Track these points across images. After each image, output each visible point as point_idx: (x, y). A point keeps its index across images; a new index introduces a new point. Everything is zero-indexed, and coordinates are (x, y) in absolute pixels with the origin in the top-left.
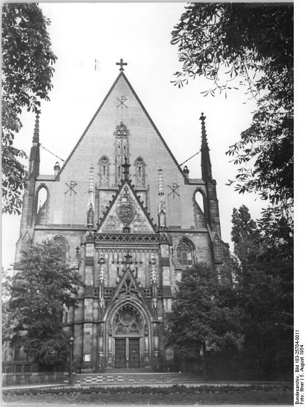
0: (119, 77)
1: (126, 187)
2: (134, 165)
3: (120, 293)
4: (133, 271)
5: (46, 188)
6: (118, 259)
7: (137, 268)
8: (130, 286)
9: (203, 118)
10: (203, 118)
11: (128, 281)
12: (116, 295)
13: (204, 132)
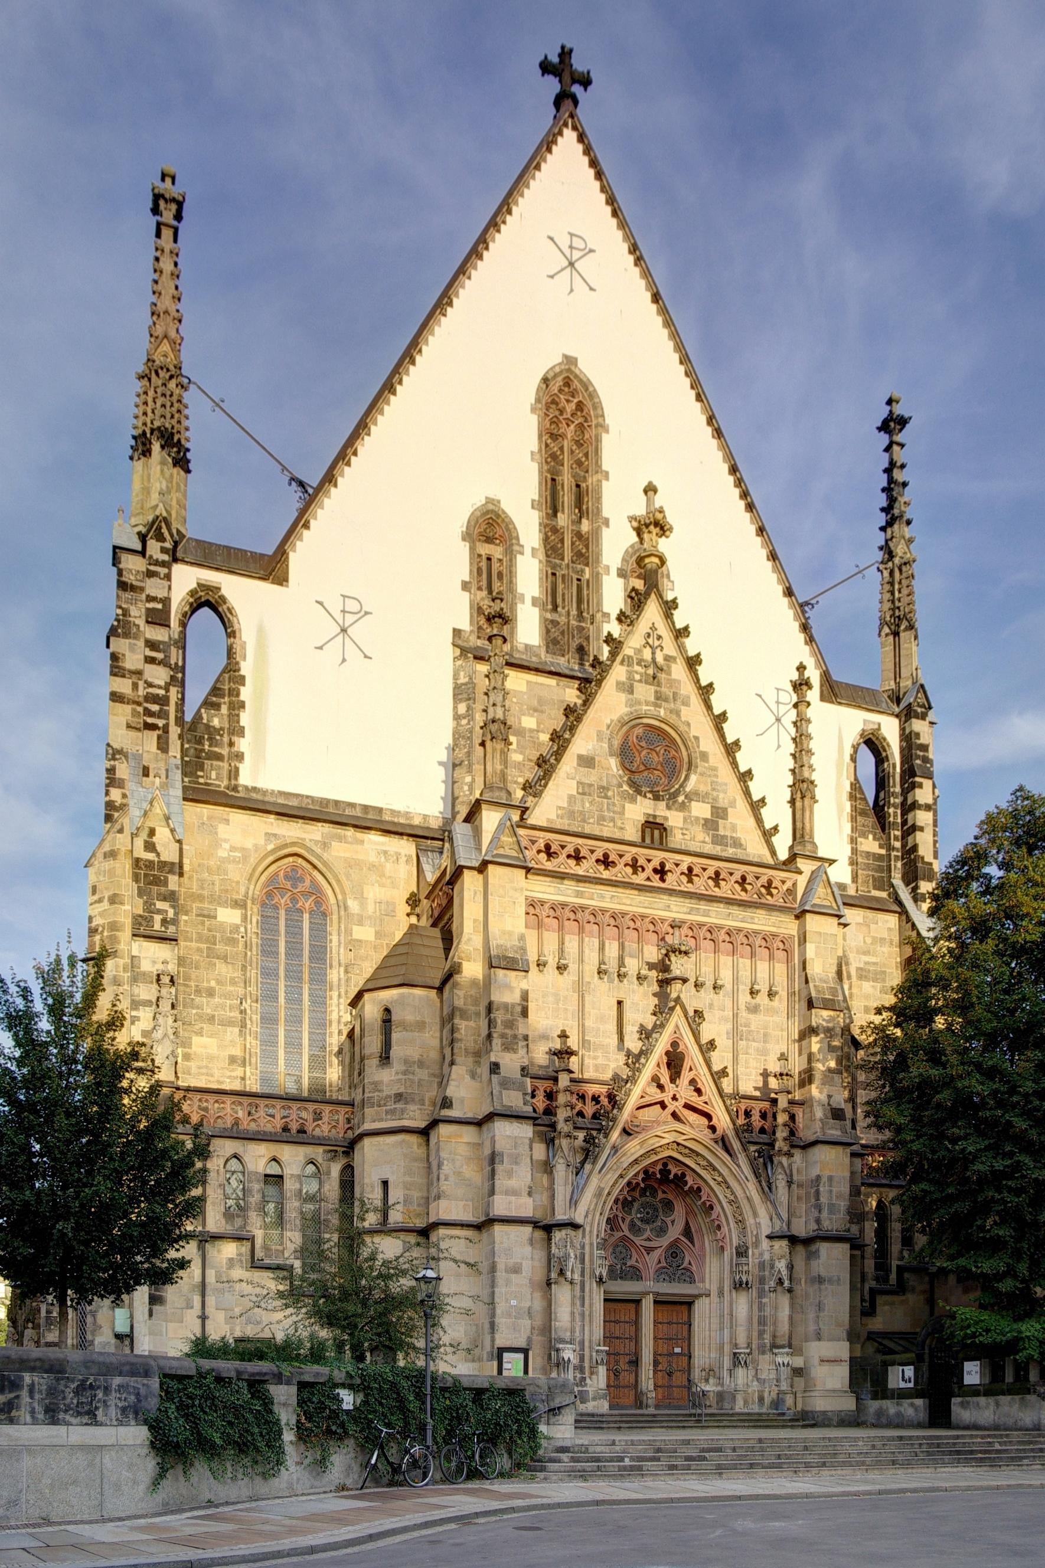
6: (621, 963)
11: (674, 1061)
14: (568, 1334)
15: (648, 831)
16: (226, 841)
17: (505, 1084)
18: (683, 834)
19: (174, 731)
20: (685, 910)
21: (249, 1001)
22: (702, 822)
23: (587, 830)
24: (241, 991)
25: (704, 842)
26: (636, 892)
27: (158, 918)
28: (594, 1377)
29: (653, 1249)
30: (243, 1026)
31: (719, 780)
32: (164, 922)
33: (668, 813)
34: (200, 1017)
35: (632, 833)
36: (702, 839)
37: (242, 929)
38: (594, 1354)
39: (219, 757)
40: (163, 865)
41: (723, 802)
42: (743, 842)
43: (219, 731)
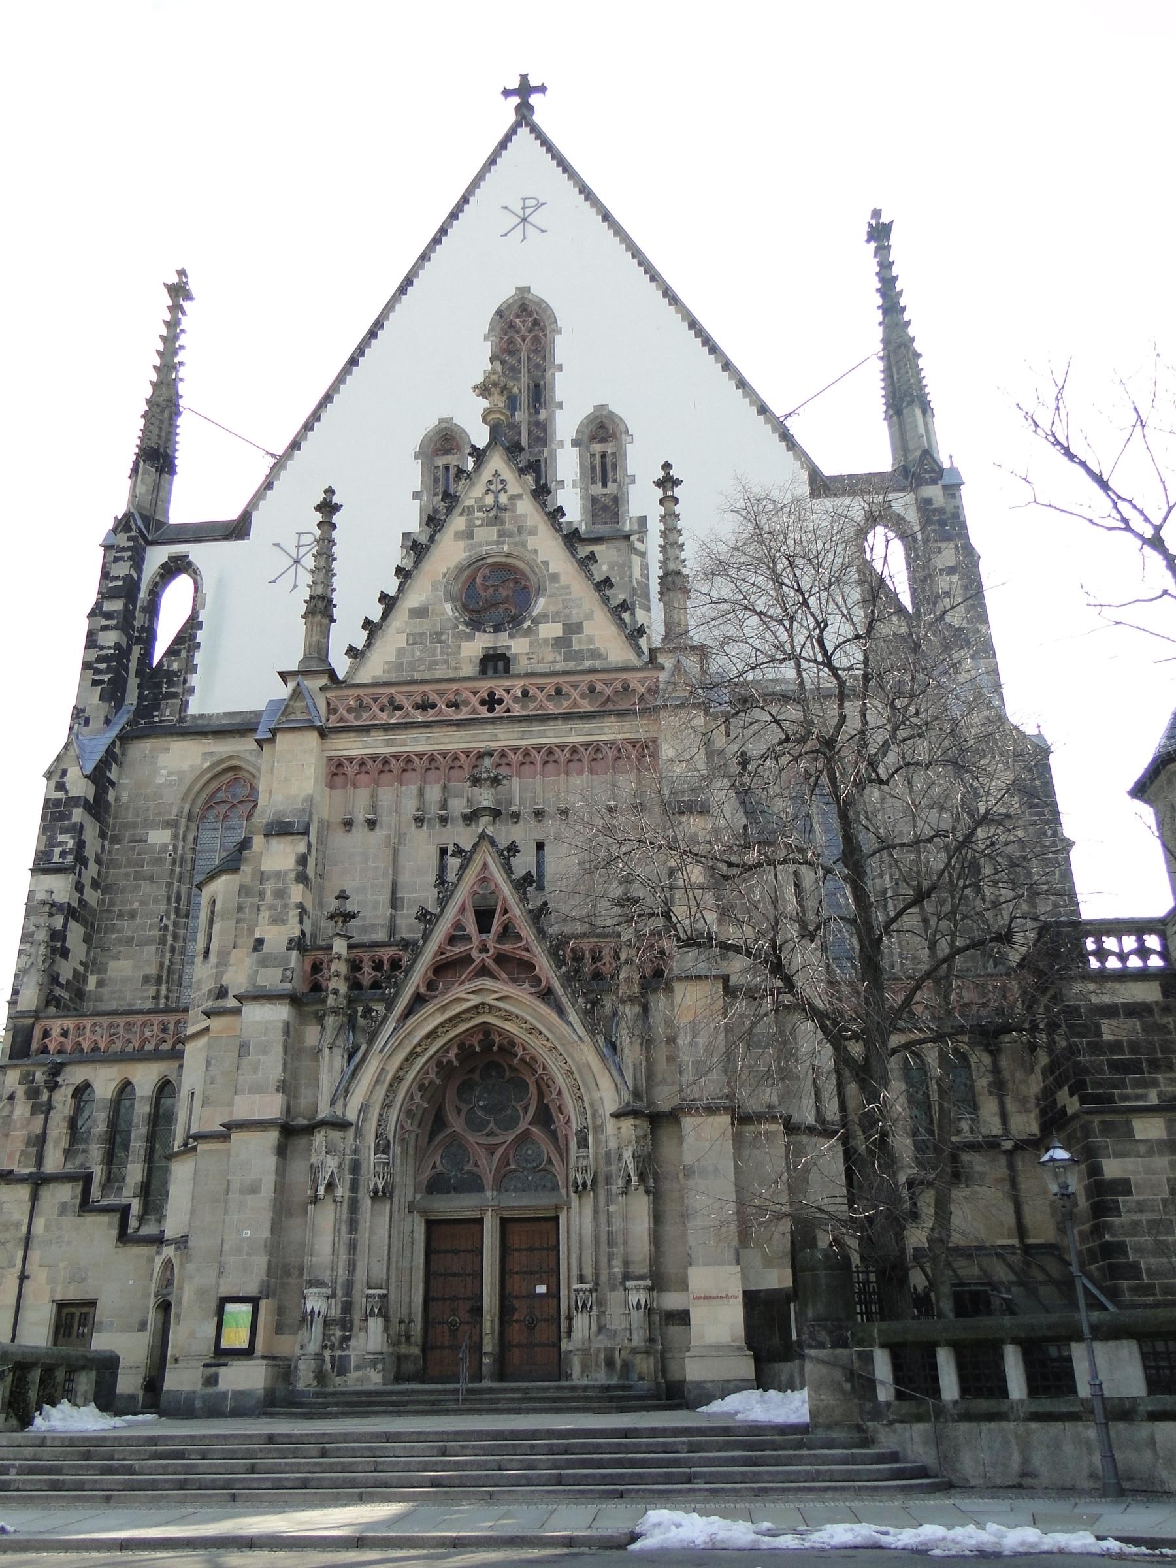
0: (513, 131)
1: (496, 474)
2: (575, 443)
3: (443, 969)
4: (513, 849)
5: (195, 574)
6: (444, 805)
7: (540, 846)
8: (496, 926)
9: (880, 233)
10: (880, 233)
12: (416, 980)
13: (892, 308)
14: (328, 1273)
15: (490, 665)
16: (164, 768)
17: (264, 963)
18: (529, 659)
19: (133, 682)
20: (516, 735)
21: (173, 917)
22: (552, 642)
23: (417, 676)
24: (162, 908)
25: (554, 662)
26: (455, 728)
27: (57, 851)
28: (362, 1334)
29: (498, 1145)
30: (163, 942)
31: (573, 596)
32: (63, 854)
33: (511, 643)
34: (119, 941)
35: (469, 669)
36: (550, 657)
37: (171, 847)
38: (364, 1300)
39: (175, 695)
40: (69, 799)
41: (576, 615)
42: (603, 651)
43: (175, 674)
